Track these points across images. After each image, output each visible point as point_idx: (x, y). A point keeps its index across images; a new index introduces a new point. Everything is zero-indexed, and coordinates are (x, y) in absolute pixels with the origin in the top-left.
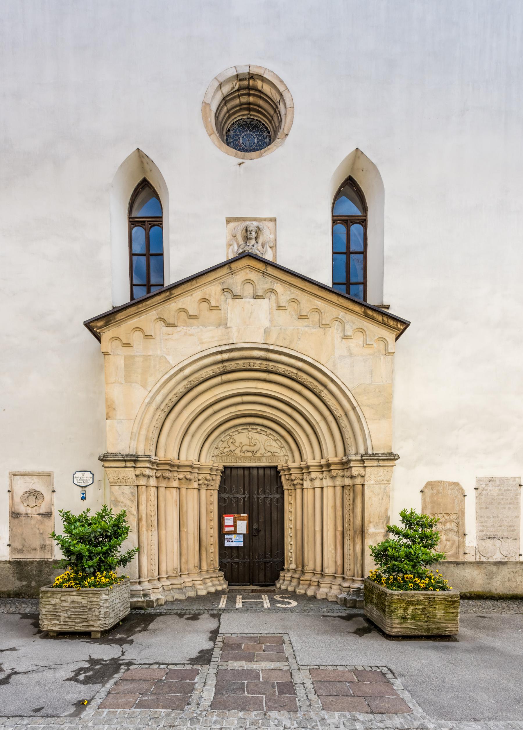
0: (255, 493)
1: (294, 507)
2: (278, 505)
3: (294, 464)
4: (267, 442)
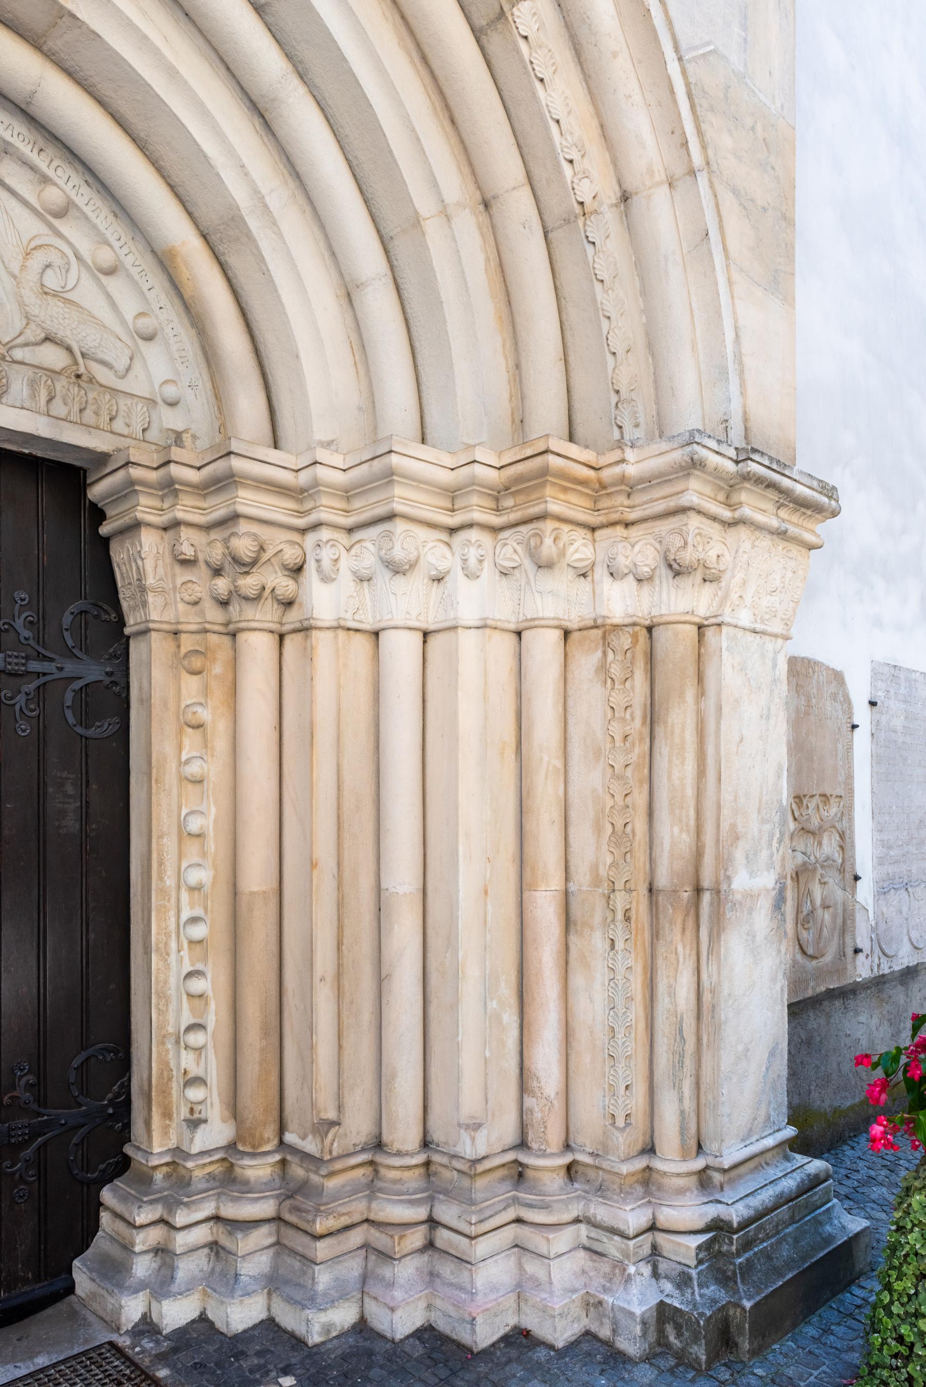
1: (221, 744)
3: (273, 455)
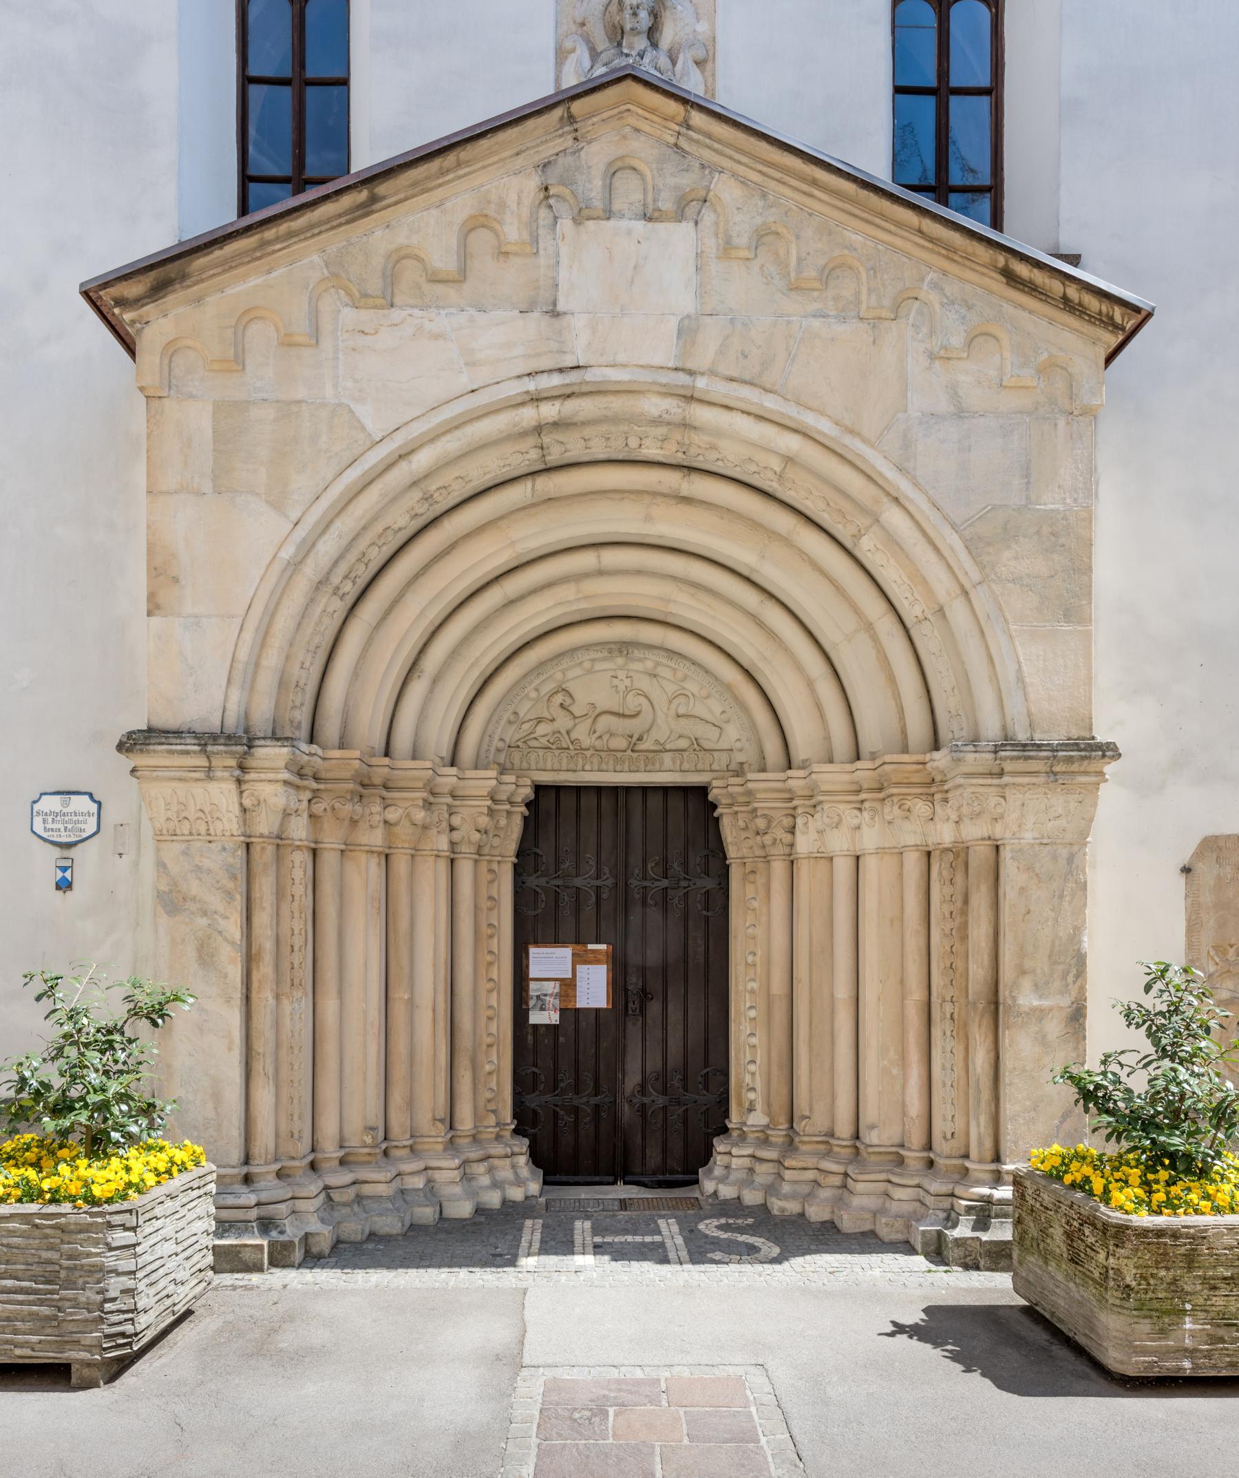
0: (636, 871)
1: (764, 919)
2: (710, 914)
4: (675, 702)
